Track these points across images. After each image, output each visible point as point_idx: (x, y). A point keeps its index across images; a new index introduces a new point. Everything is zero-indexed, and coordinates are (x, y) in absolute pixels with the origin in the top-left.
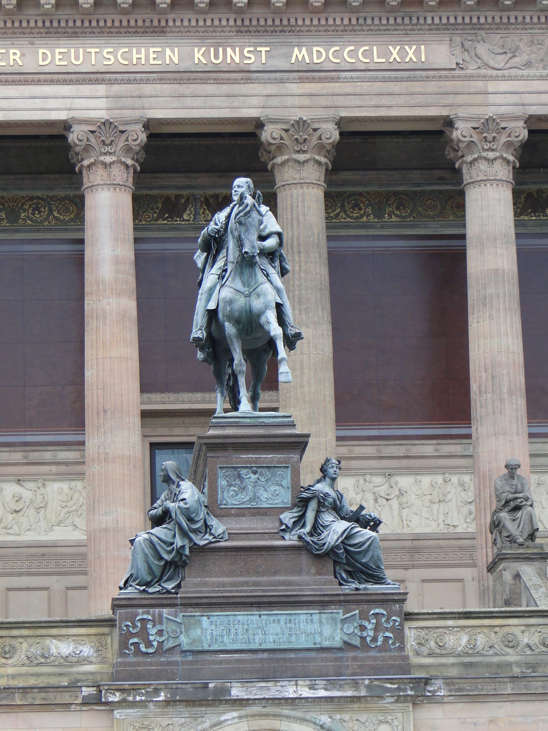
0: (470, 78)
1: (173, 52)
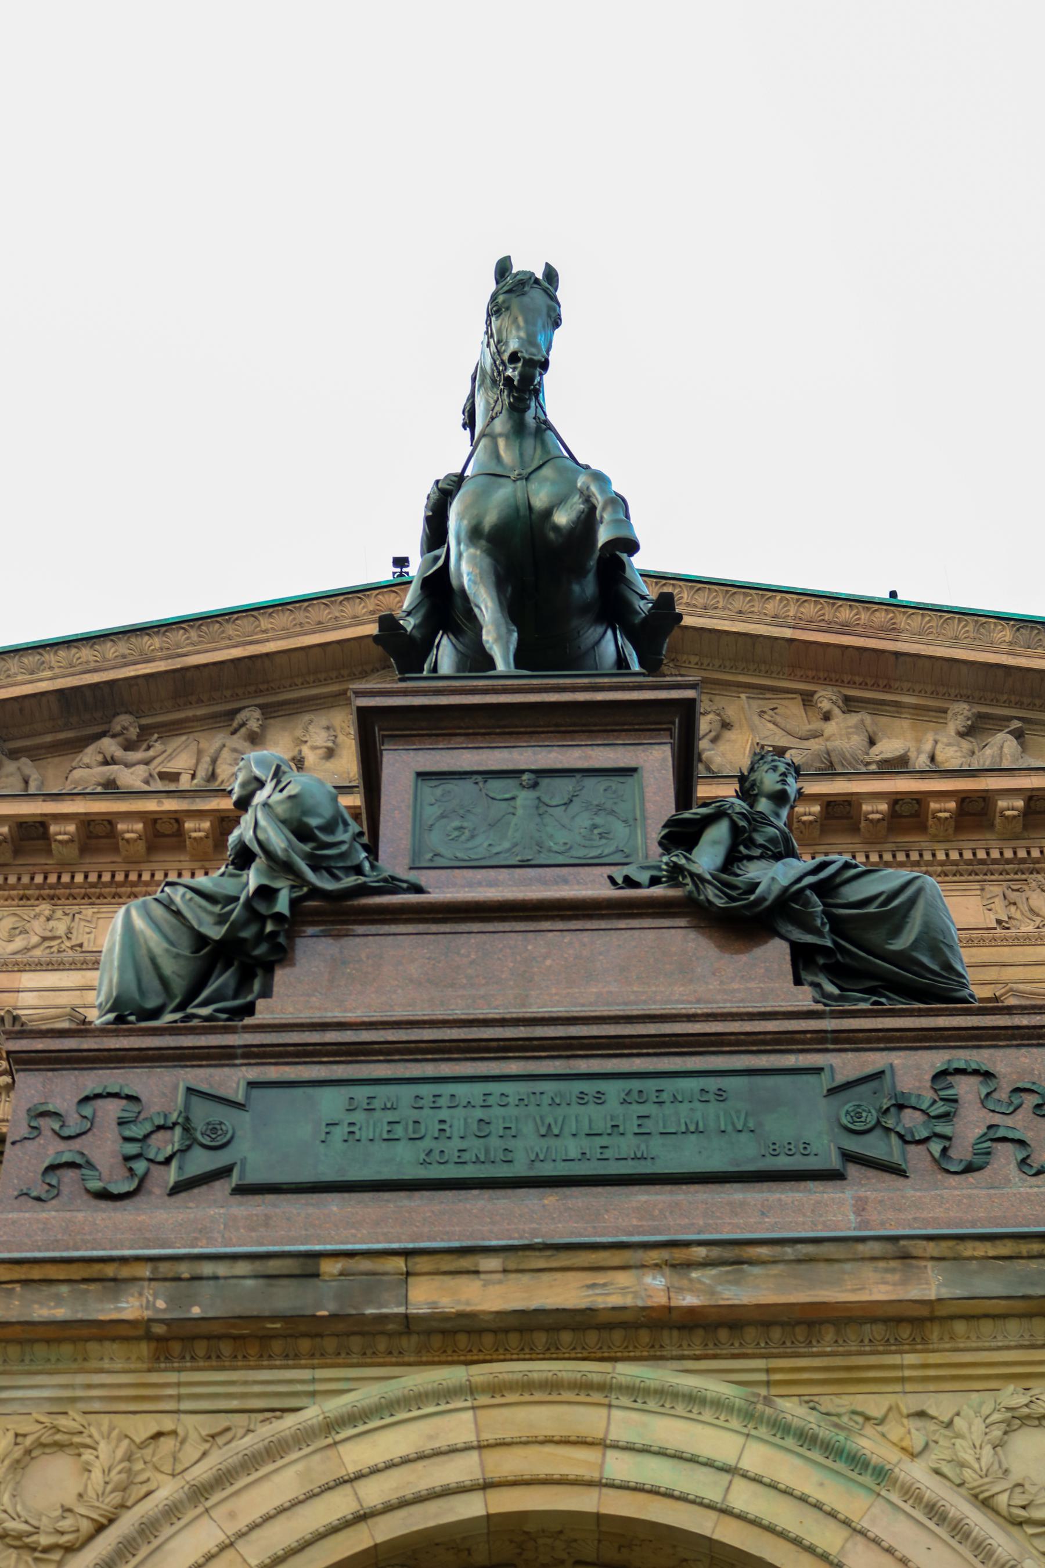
0: (1025, 941)
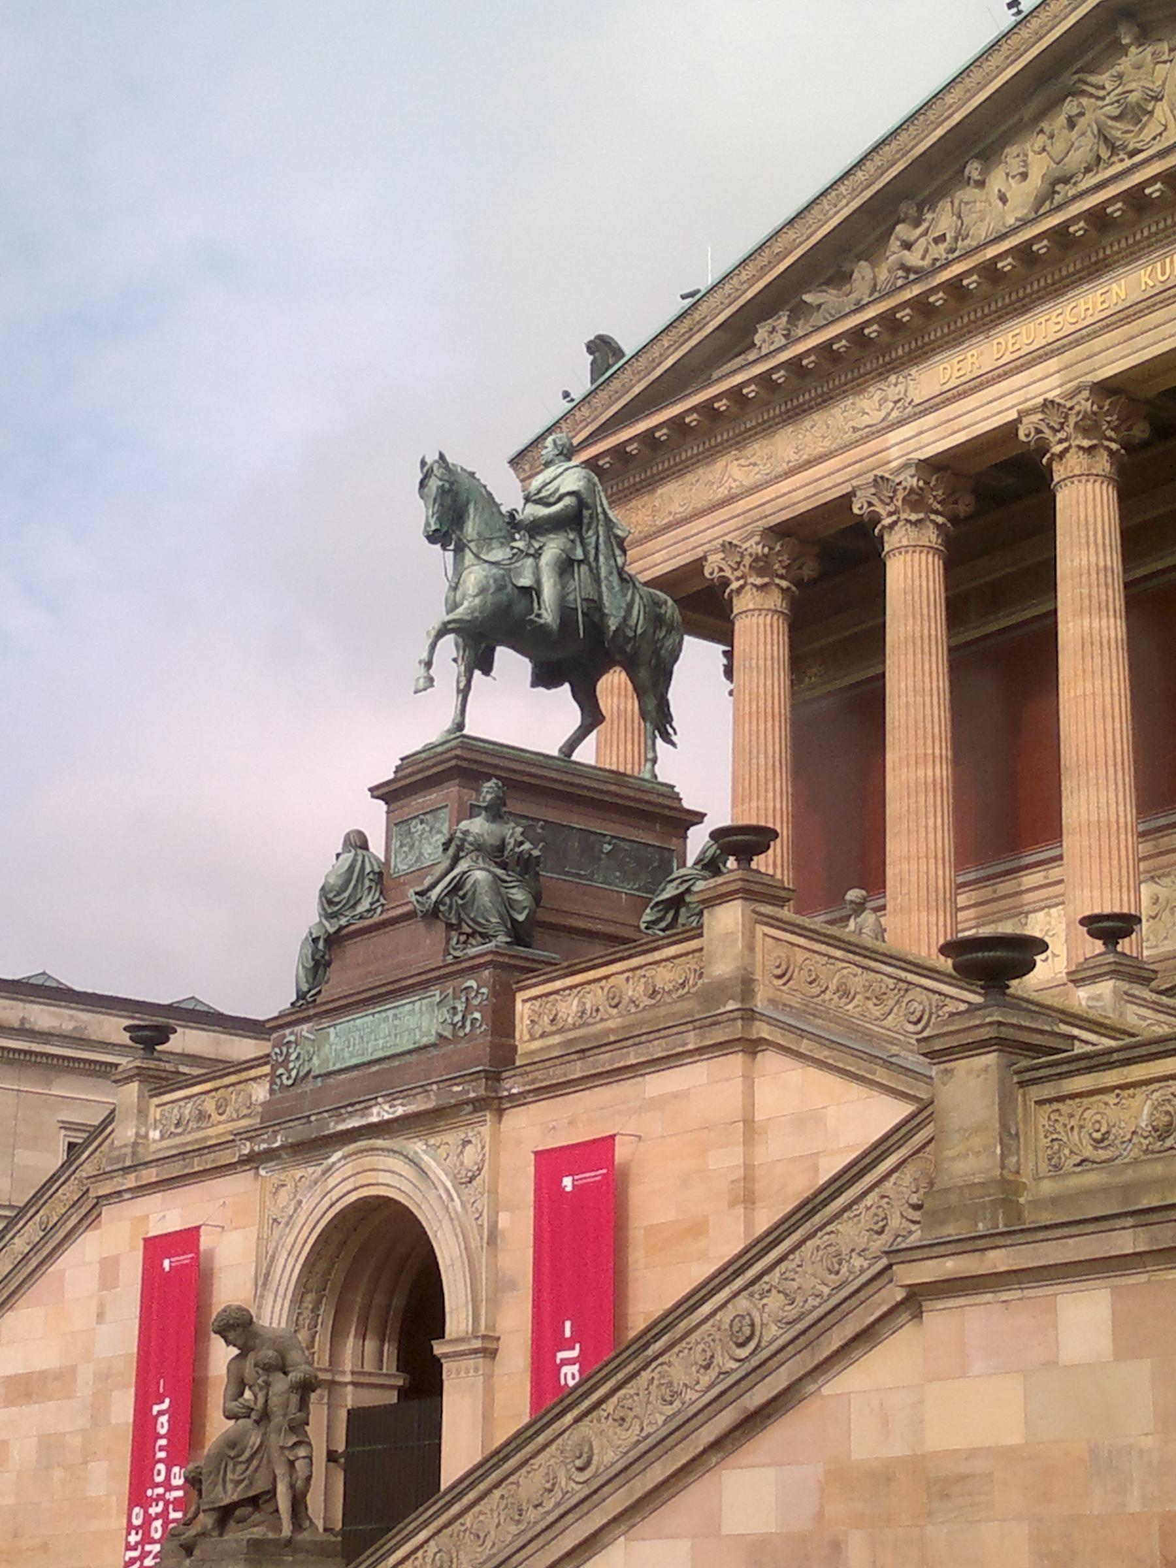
1: (1120, 286)
